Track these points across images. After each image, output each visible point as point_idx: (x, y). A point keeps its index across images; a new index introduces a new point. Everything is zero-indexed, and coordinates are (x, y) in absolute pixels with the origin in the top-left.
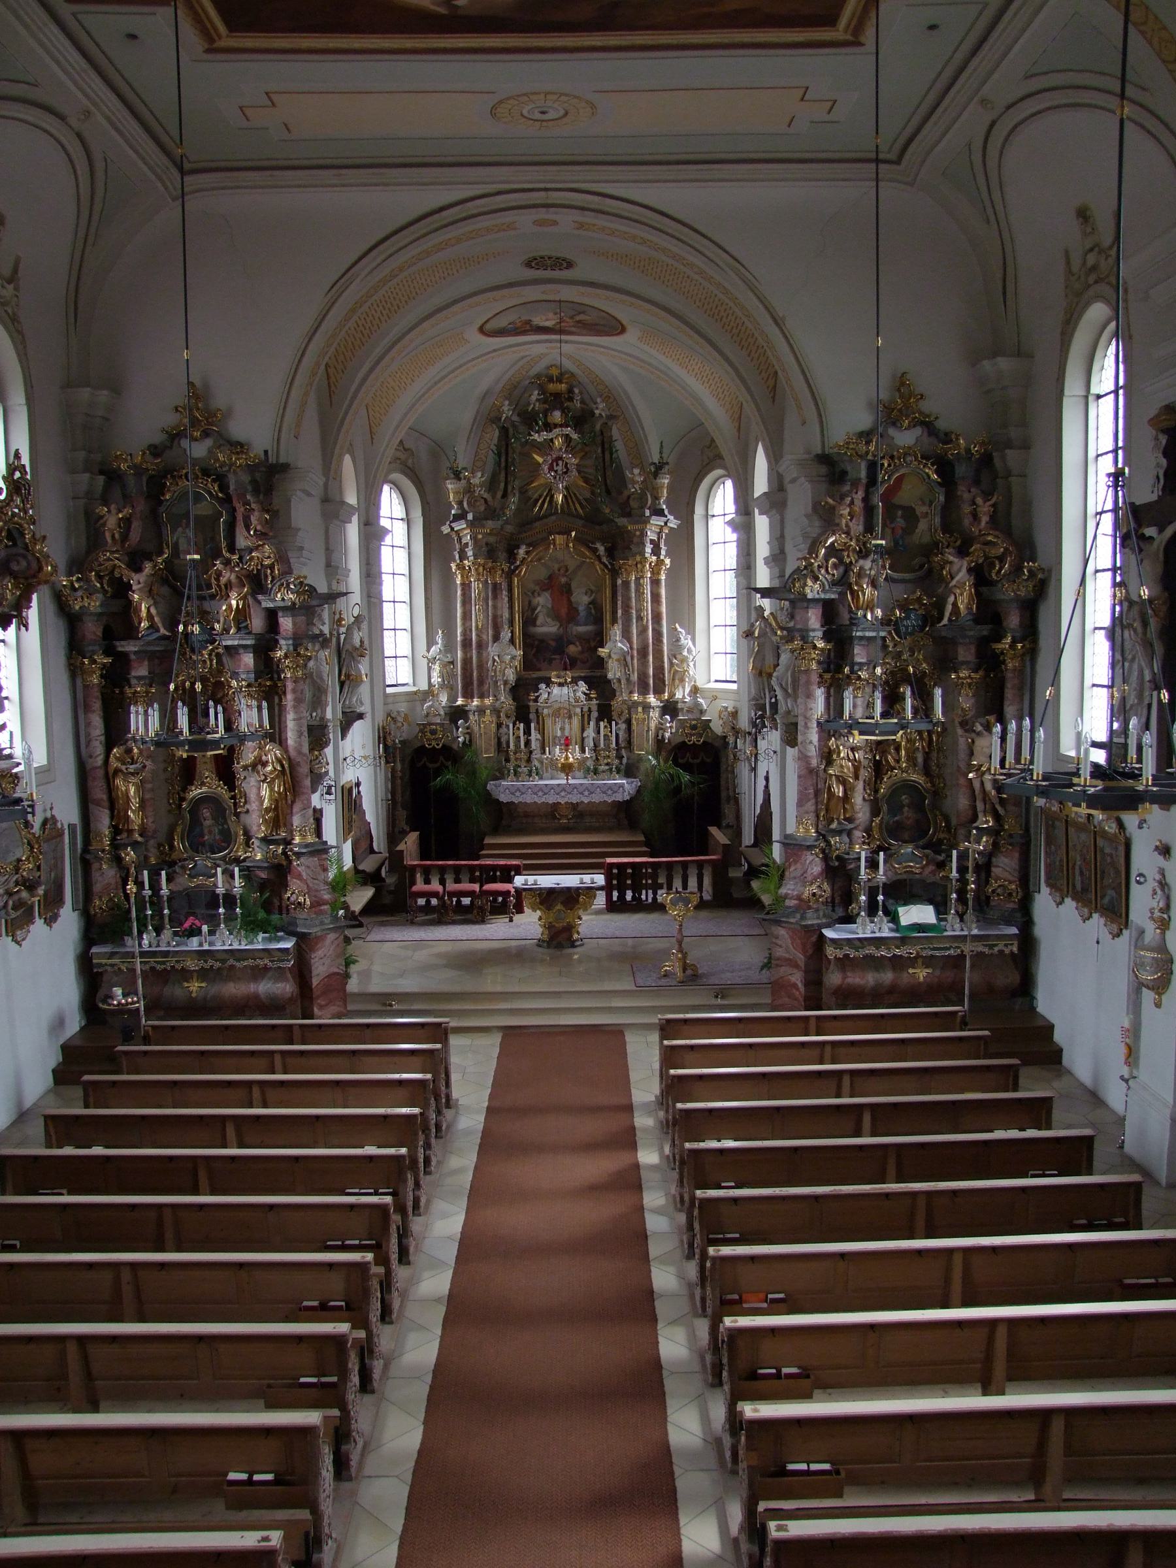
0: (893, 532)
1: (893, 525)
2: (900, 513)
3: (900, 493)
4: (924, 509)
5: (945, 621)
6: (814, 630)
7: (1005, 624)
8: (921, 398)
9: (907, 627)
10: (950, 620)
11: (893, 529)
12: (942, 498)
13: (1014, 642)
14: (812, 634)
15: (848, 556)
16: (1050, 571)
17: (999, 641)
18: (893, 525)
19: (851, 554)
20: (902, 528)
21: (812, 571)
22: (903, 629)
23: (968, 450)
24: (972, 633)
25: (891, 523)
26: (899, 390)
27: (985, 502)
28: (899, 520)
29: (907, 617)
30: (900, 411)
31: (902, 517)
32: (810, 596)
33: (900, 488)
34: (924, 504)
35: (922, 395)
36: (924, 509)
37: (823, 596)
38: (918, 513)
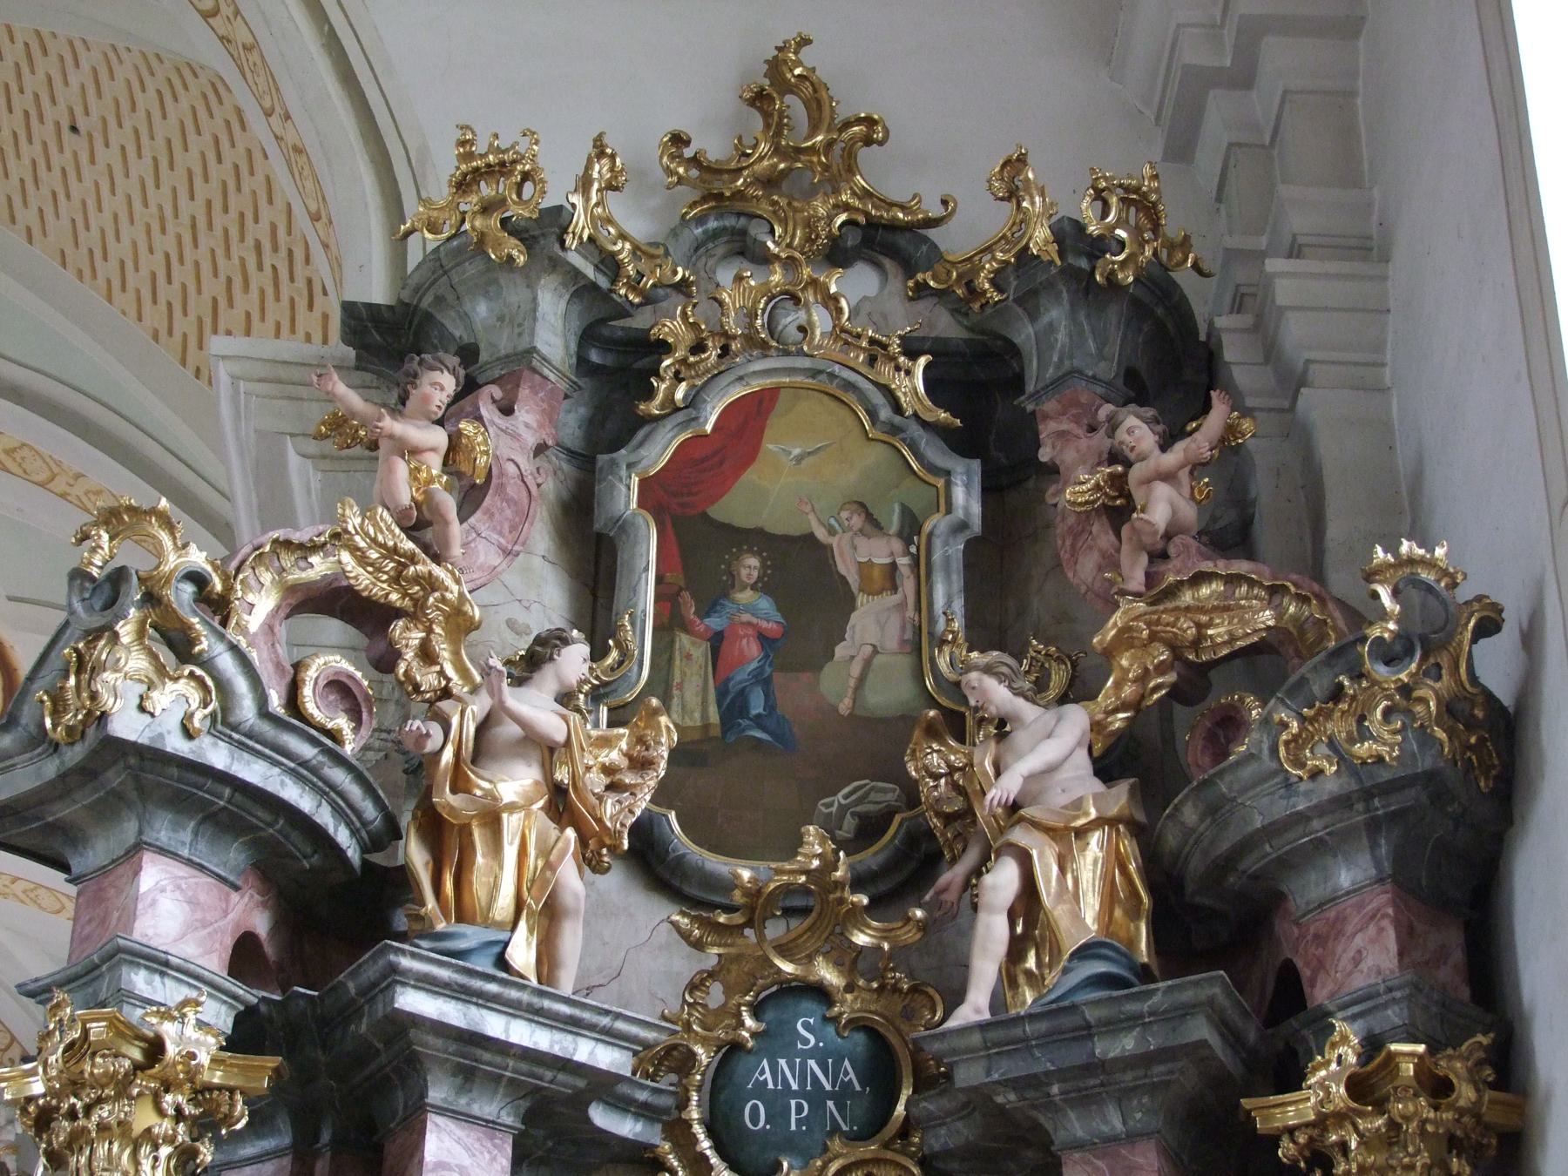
0: (715, 653)
1: (715, 622)
2: (750, 566)
3: (750, 476)
4: (881, 551)
5: (975, 1007)
6: (160, 964)
7: (1320, 994)
8: (868, 141)
9: (777, 1102)
10: (997, 1003)
11: (717, 642)
12: (966, 498)
13: (1372, 1045)
14: (140, 981)
15: (427, 654)
16: (1531, 639)
17: (1289, 1077)
18: (715, 622)
19: (443, 650)
20: (764, 639)
21: (151, 599)
22: (755, 1116)
23: (1069, 234)
24: (1128, 1043)
25: (708, 609)
26: (759, 100)
27: (1165, 446)
28: (745, 596)
29: (775, 1040)
30: (770, 182)
31: (764, 586)
32: (127, 725)
33: (750, 456)
34: (874, 524)
35: (870, 122)
36: (881, 551)
37: (219, 756)
38: (846, 568)
